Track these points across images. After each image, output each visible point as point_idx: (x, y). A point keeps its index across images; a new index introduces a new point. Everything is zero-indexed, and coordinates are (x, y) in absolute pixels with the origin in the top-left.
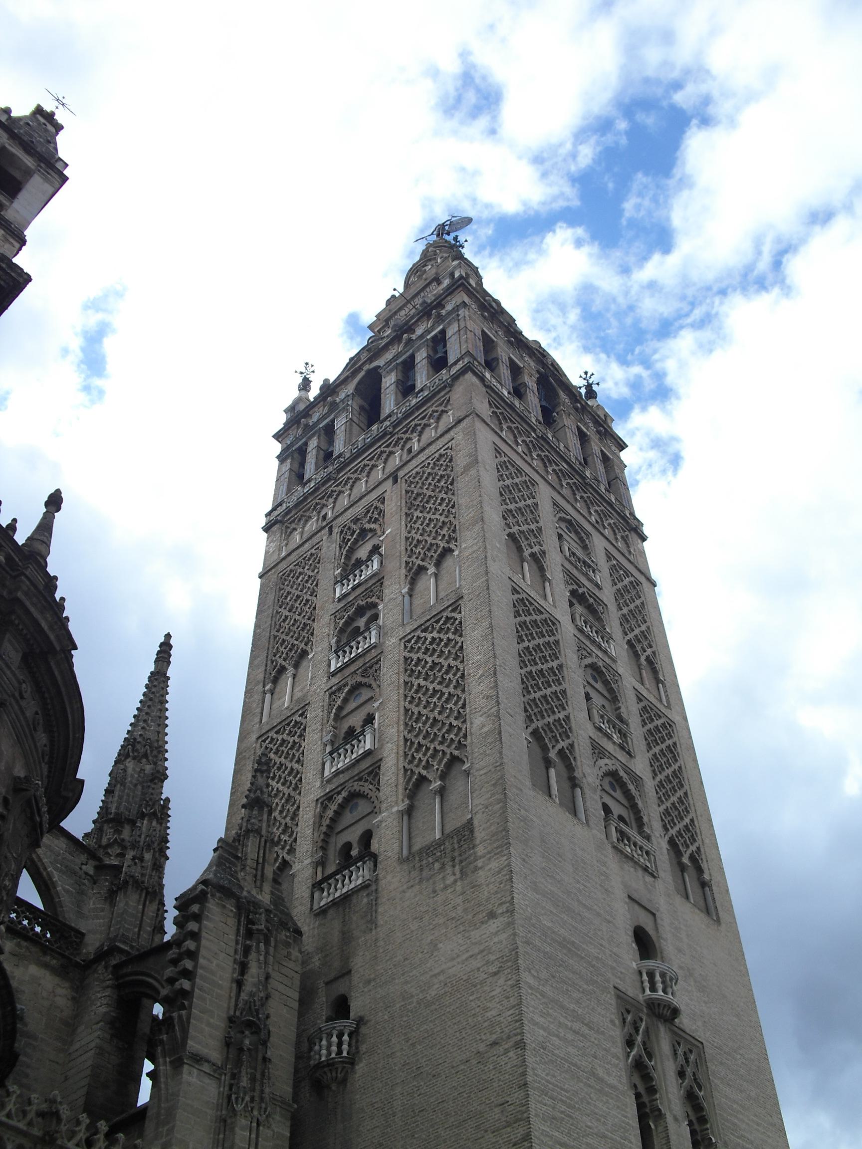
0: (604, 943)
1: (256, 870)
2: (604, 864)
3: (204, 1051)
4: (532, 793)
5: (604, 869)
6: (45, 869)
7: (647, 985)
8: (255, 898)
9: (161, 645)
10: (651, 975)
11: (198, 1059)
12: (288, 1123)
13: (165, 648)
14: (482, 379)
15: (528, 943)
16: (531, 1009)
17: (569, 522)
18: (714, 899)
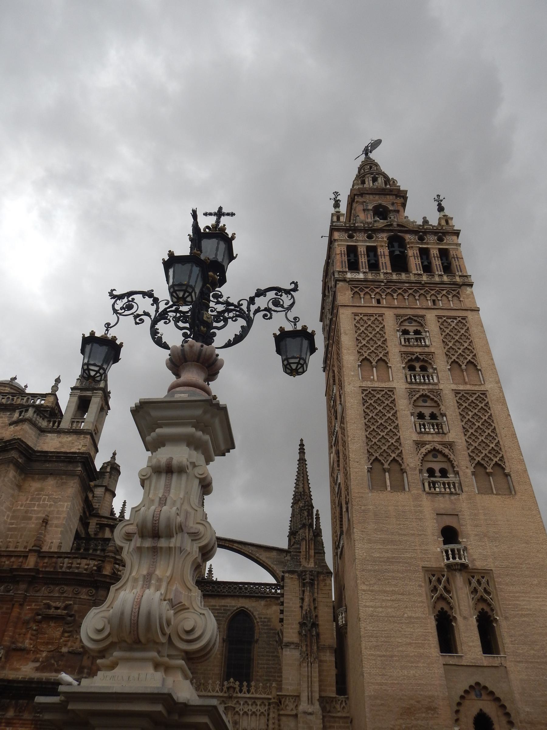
0: (416, 548)
1: (306, 555)
2: (420, 506)
3: (290, 640)
4: (370, 495)
5: (419, 508)
6: (270, 567)
7: (445, 557)
8: (306, 567)
9: (300, 445)
10: (447, 552)
11: (288, 645)
12: (334, 654)
13: (302, 445)
14: (344, 280)
15: (363, 570)
16: (364, 601)
17: (410, 318)
18: (512, 481)
